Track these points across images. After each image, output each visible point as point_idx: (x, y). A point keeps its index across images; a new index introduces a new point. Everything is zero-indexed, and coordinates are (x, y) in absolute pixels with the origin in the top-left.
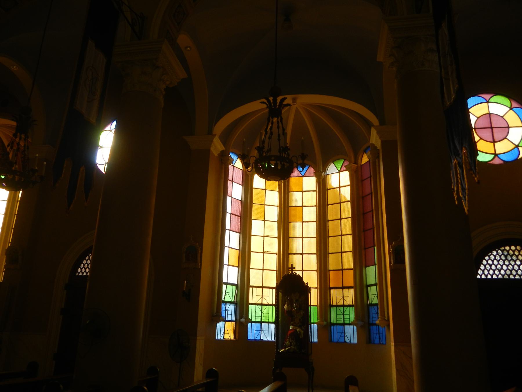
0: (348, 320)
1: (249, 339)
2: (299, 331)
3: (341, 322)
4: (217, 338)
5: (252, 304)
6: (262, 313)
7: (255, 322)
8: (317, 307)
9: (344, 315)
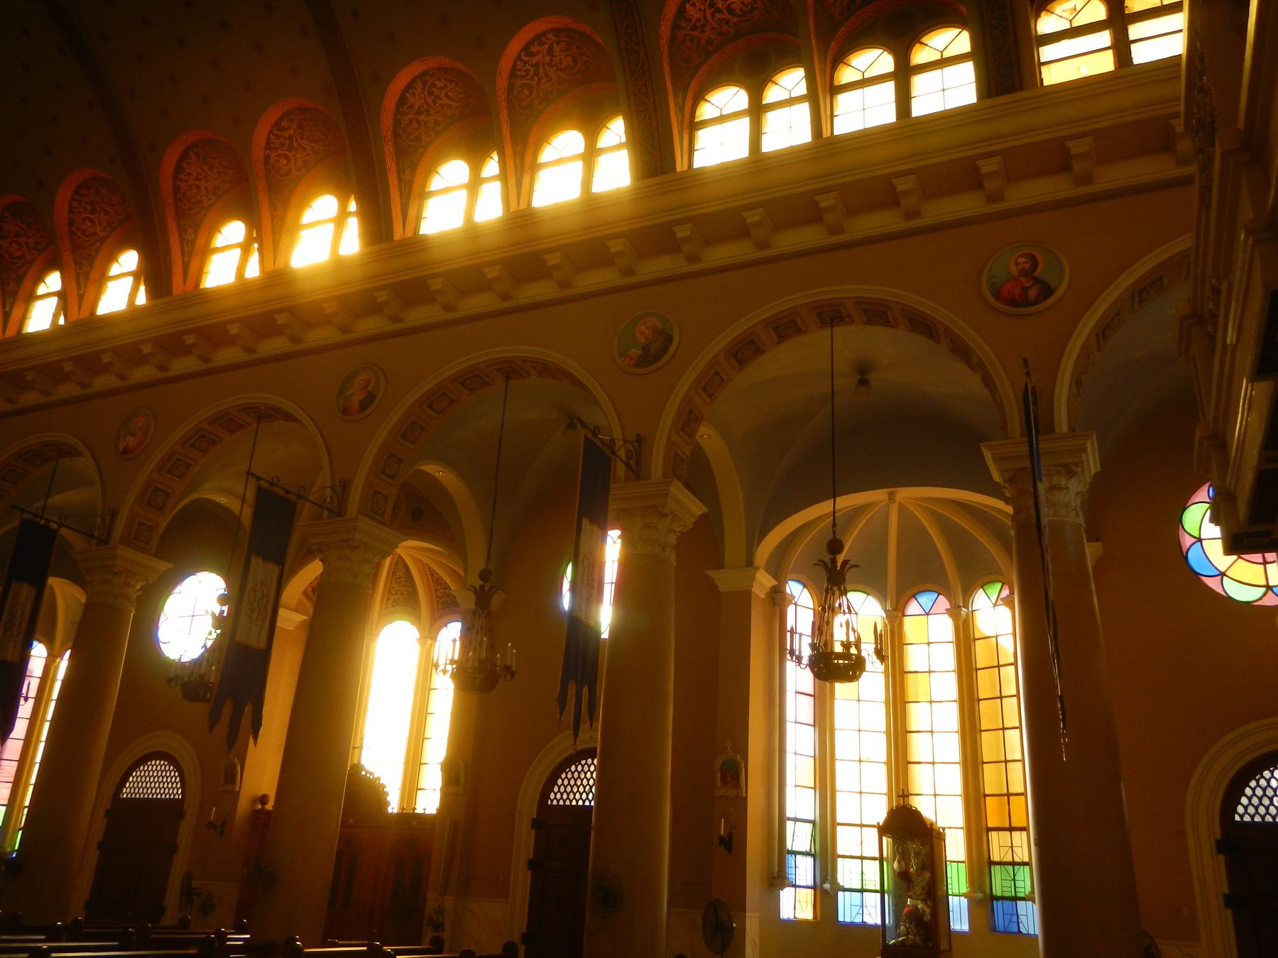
2: (922, 909)
3: (1009, 894)
8: (964, 864)
9: (1014, 880)
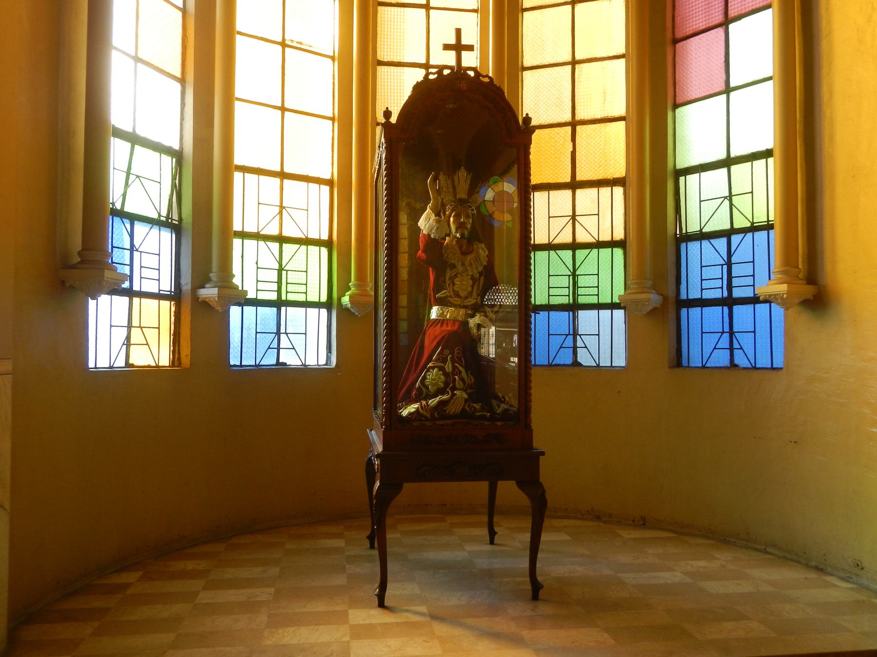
0: (595, 291)
1: (235, 366)
3: (564, 300)
4: (91, 364)
5: (243, 235)
6: (280, 270)
7: (256, 303)
